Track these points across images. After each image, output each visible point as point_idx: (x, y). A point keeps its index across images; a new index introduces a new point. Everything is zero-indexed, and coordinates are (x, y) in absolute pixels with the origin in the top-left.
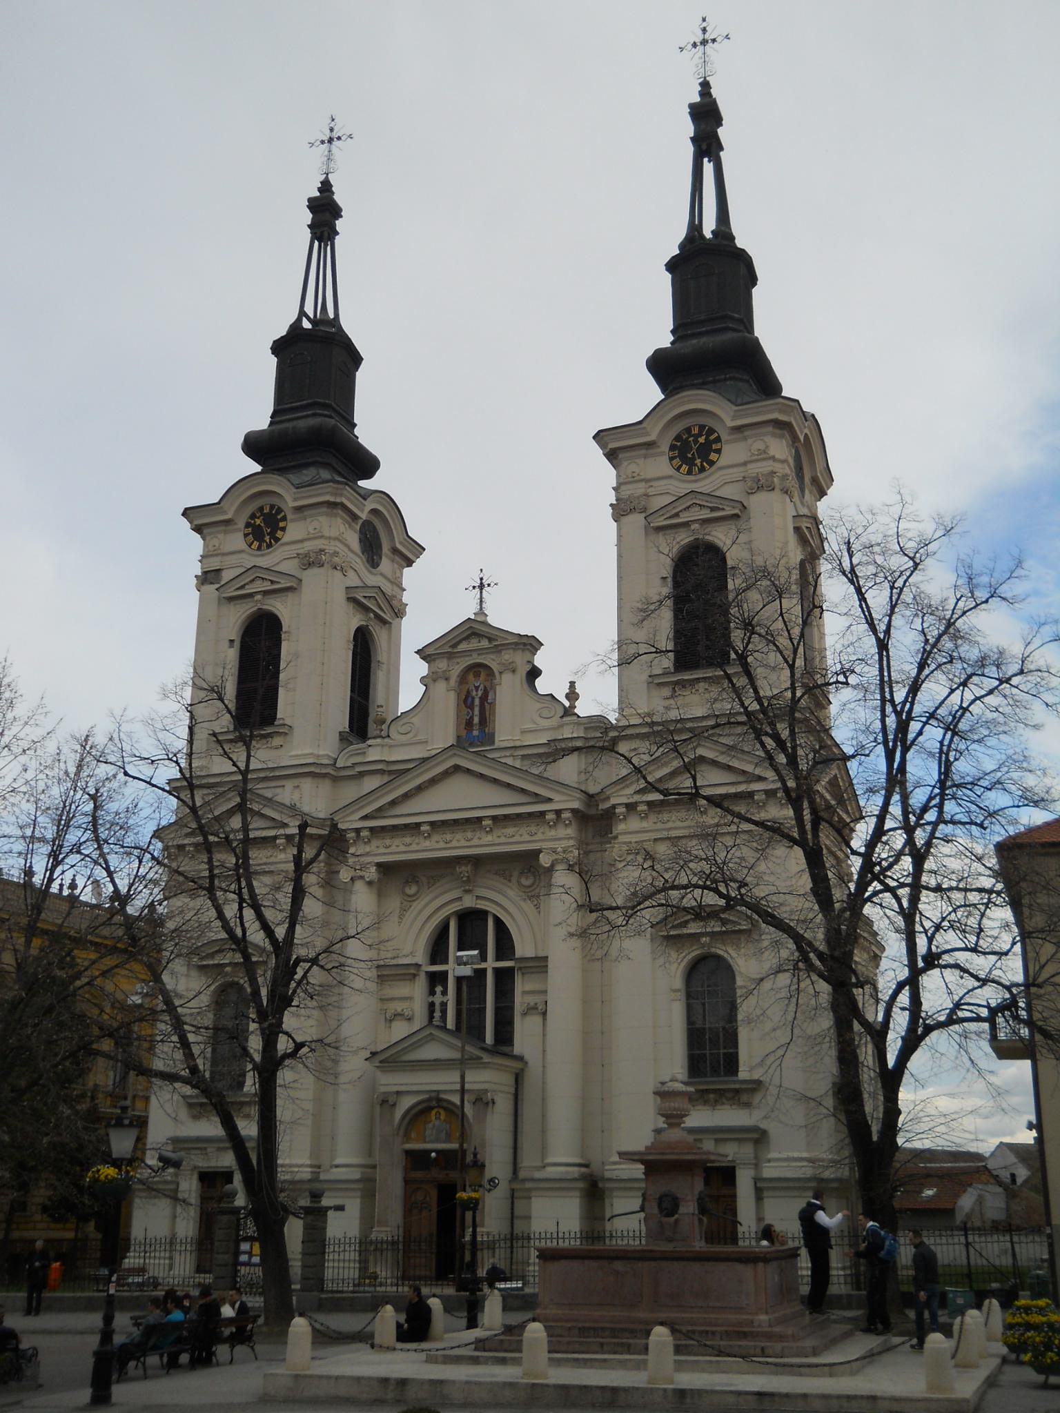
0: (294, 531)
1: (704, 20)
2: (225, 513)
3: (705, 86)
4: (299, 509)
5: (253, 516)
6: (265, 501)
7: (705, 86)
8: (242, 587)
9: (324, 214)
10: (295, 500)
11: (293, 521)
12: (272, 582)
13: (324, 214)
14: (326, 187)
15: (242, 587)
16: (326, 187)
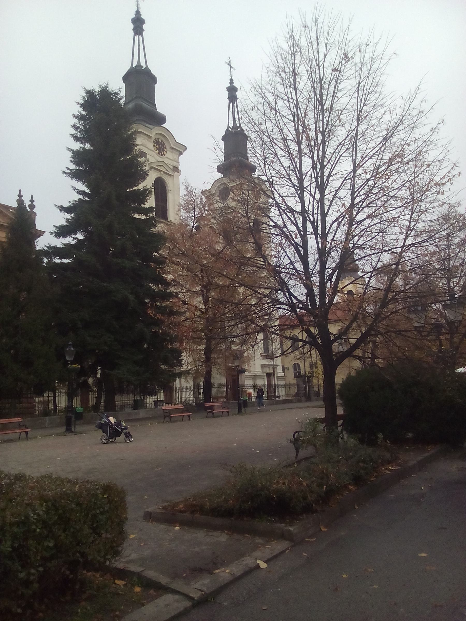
0: (169, 154)
1: (229, 58)
2: (151, 133)
3: (231, 80)
4: (172, 148)
5: (155, 139)
6: (161, 138)
7: (231, 80)
8: (157, 166)
9: (138, 23)
10: (174, 145)
11: (169, 151)
12: (167, 170)
13: (138, 23)
14: (138, 13)
15: (157, 166)
16: (138, 13)
